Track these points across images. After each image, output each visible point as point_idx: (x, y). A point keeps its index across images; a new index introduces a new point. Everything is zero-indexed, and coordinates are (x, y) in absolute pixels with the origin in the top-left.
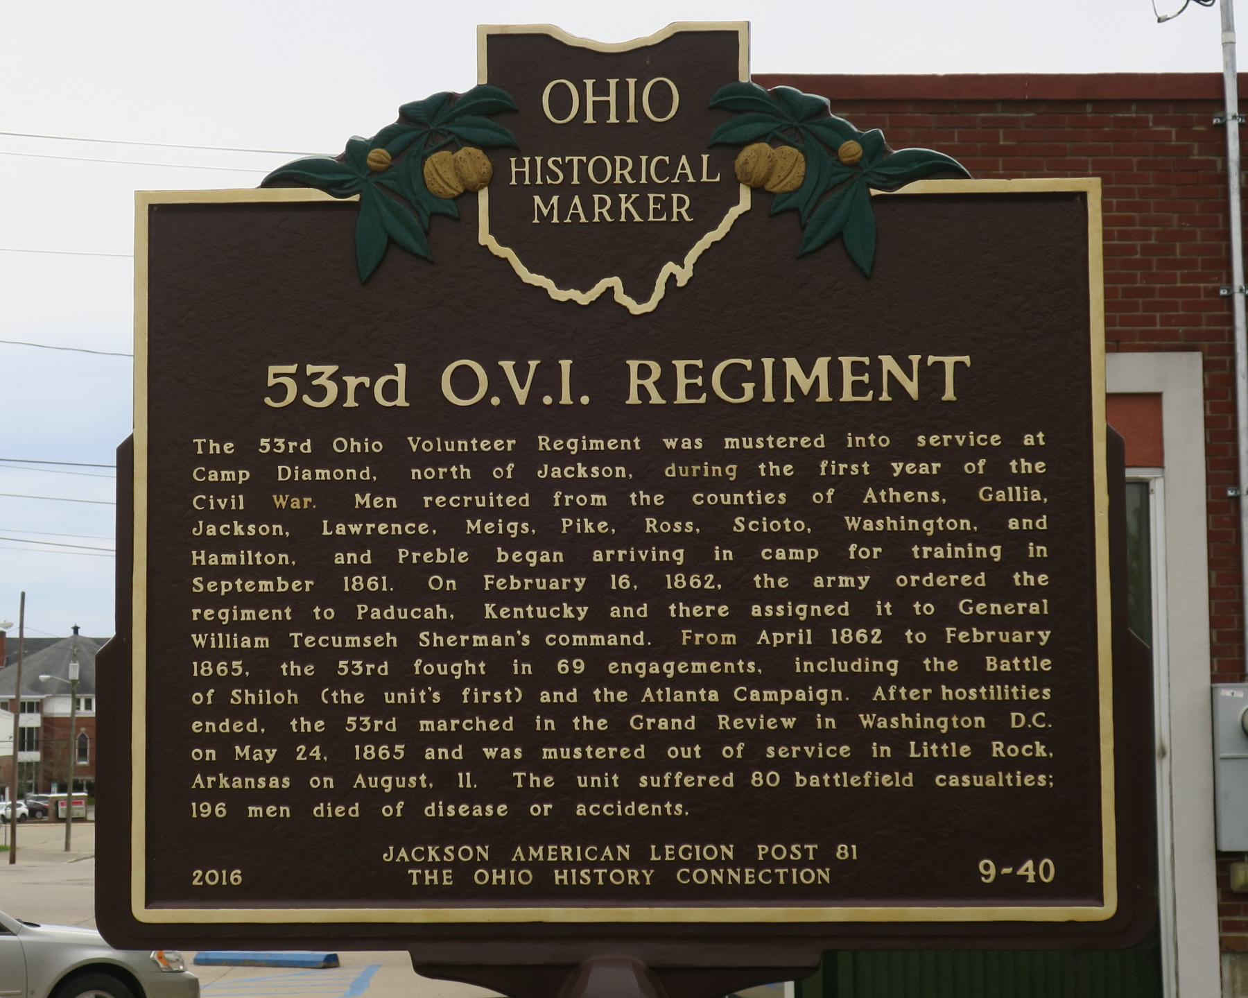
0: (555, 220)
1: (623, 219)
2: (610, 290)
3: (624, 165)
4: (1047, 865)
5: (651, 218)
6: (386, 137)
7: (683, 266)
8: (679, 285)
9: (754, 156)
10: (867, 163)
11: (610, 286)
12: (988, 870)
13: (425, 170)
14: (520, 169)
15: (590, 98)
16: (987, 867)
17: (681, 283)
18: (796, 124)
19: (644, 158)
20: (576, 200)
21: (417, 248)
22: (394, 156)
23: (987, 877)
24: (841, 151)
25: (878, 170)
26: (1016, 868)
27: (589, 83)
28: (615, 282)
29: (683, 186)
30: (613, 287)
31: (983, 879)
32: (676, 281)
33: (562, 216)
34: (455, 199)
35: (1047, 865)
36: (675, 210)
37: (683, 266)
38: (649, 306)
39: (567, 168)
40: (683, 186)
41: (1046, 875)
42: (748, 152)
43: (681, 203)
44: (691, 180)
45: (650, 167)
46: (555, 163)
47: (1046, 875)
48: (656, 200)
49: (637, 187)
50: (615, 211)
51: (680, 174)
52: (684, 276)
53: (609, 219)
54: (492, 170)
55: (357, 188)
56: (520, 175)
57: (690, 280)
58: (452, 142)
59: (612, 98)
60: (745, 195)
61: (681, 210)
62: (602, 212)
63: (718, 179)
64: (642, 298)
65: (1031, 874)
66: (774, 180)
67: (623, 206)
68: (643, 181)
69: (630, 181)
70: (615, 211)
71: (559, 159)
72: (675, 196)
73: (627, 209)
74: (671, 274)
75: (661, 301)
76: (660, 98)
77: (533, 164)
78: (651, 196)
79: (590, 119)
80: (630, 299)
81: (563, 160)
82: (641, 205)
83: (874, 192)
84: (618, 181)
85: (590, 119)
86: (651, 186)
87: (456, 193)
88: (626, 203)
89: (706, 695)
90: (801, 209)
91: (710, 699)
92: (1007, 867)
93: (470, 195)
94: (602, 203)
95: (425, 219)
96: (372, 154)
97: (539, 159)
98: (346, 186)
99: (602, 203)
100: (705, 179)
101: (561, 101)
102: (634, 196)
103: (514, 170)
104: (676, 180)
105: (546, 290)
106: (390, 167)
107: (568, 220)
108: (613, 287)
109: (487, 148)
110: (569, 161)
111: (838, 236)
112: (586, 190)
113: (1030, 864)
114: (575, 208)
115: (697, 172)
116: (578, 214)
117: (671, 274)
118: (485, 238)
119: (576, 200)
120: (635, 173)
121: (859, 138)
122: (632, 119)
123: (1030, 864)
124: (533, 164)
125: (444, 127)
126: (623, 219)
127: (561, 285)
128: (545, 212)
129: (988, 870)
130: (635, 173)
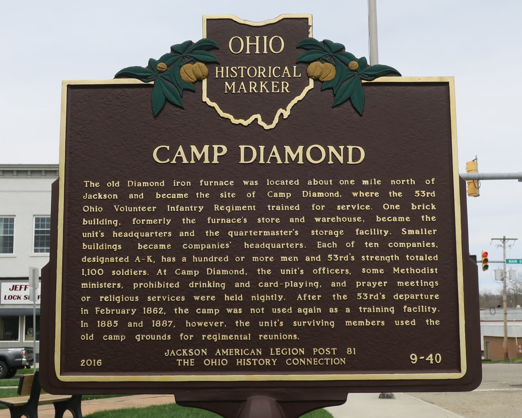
0: (234, 92)
1: (261, 91)
2: (256, 119)
3: (262, 70)
4: (438, 356)
5: (273, 91)
6: (164, 58)
7: (286, 110)
8: (284, 117)
9: (316, 68)
10: (360, 70)
11: (256, 118)
12: (414, 358)
13: (181, 71)
14: (220, 71)
15: (248, 44)
16: (413, 357)
17: (285, 117)
18: (331, 54)
19: (270, 67)
20: (242, 83)
21: (177, 103)
22: (168, 66)
23: (414, 361)
24: (350, 65)
25: (363, 73)
26: (426, 357)
27: (248, 38)
28: (258, 116)
29: (286, 79)
30: (257, 118)
31: (412, 362)
32: (283, 116)
33: (237, 89)
34: (194, 83)
35: (438, 356)
36: (283, 88)
37: (286, 110)
38: (273, 126)
39: (239, 71)
40: (286, 79)
41: (438, 360)
42: (313, 65)
43: (285, 85)
44: (289, 76)
45: (272, 71)
46: (234, 69)
47: (438, 360)
48: (275, 84)
49: (267, 79)
50: (258, 88)
51: (285, 74)
52: (286, 114)
53: (256, 91)
54: (208, 72)
55: (152, 79)
56: (220, 74)
57: (289, 116)
58: (192, 61)
59: (257, 44)
60: (311, 81)
61: (285, 88)
62: (253, 88)
63: (300, 76)
64: (269, 122)
65: (432, 360)
66: (322, 76)
67: (262, 86)
68: (270, 76)
69: (264, 76)
70: (258, 88)
71: (236, 68)
72: (283, 83)
73: (263, 87)
74: (281, 113)
75: (277, 124)
76: (276, 44)
77: (225, 69)
78: (273, 82)
79: (248, 52)
80: (264, 123)
81: (237, 68)
82: (269, 86)
83: (363, 81)
84: (259, 76)
85: (248, 52)
86: (273, 78)
87: (193, 81)
88: (263, 85)
89: (419, 258)
90: (334, 88)
91: (420, 259)
92: (422, 356)
93: (199, 81)
94: (253, 85)
95: (181, 92)
96: (159, 65)
97: (227, 68)
98: (148, 78)
99: (253, 85)
100: (295, 76)
101: (236, 44)
102: (266, 82)
103: (217, 72)
104: (283, 76)
105: (230, 120)
106: (167, 70)
107: (239, 92)
108: (257, 118)
109: (206, 63)
110: (239, 68)
111: (349, 99)
112: (246, 80)
113: (431, 356)
114: (242, 87)
115: (292, 73)
116: (243, 89)
117: (281, 113)
118: (205, 98)
119: (242, 83)
120: (267, 73)
121: (357, 60)
122: (265, 52)
123: (431, 356)
124: (225, 69)
125: (189, 54)
126: (261, 91)
127: (236, 118)
128: (230, 89)
129: (414, 358)
130: (267, 73)
